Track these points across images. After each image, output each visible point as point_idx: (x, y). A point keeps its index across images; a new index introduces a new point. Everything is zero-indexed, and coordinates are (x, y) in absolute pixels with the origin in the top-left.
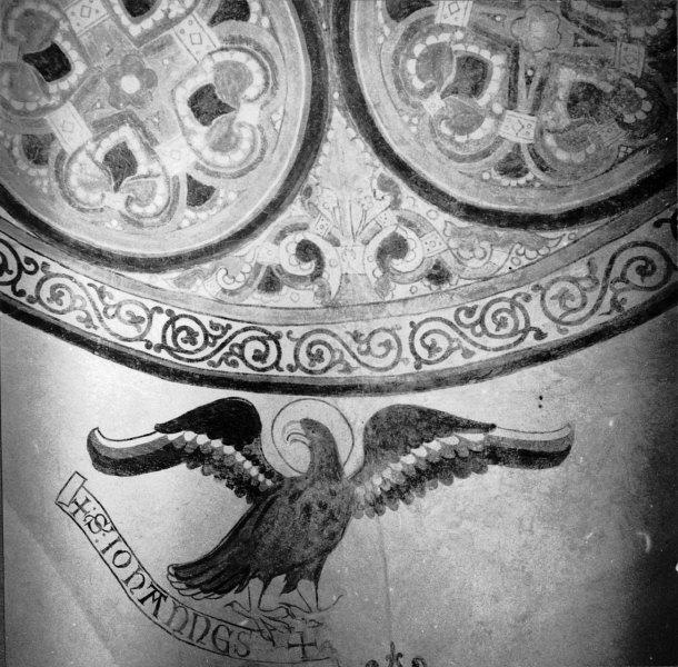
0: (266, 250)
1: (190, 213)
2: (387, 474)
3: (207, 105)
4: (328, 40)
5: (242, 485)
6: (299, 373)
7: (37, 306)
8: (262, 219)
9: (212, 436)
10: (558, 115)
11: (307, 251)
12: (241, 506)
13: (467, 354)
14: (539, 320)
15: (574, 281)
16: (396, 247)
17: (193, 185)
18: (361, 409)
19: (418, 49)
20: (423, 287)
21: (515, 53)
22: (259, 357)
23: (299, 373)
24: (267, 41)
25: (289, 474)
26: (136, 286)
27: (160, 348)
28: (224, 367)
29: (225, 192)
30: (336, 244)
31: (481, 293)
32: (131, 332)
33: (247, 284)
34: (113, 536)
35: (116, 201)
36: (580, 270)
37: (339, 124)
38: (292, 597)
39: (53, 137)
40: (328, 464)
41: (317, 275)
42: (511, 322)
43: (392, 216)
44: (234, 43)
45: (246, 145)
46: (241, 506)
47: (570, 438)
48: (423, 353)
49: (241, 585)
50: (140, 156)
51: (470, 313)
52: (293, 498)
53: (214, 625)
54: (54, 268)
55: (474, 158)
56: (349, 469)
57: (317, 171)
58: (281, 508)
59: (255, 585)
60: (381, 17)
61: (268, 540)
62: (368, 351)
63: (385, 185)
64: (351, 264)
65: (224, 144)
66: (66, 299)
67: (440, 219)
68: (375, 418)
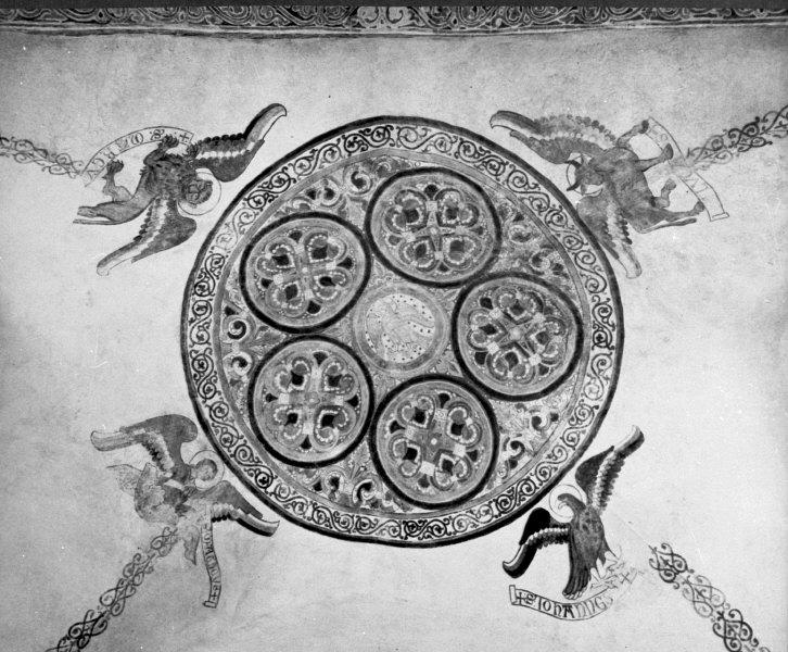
0: (505, 455)
1: (476, 464)
2: (597, 491)
3: (457, 428)
4: (472, 385)
5: (560, 539)
6: (544, 484)
10: (540, 348)
11: (515, 445)
12: (565, 547)
13: (584, 432)
14: (592, 404)
15: (589, 383)
16: (536, 421)
18: (570, 477)
19: (494, 365)
20: (554, 425)
22: (529, 489)
23: (544, 484)
24: (458, 399)
25: (569, 521)
26: (479, 500)
27: (500, 515)
28: (522, 503)
29: (480, 448)
30: (520, 435)
31: (570, 411)
32: (488, 517)
33: (507, 470)
34: (538, 599)
35: (454, 478)
36: (587, 379)
37: (493, 403)
38: (607, 563)
39: (425, 475)
40: (578, 506)
42: (586, 411)
43: (527, 414)
44: (451, 408)
46: (565, 547)
47: (638, 429)
48: (572, 444)
49: (589, 576)
51: (572, 419)
52: (577, 527)
53: (593, 599)
54: (453, 516)
55: (533, 377)
56: (585, 501)
57: (498, 420)
58: (579, 537)
59: (593, 571)
60: (479, 367)
61: (583, 550)
62: (557, 458)
63: (518, 407)
64: (529, 436)
65: (469, 436)
66: (464, 524)
67: (539, 402)
68: (577, 476)
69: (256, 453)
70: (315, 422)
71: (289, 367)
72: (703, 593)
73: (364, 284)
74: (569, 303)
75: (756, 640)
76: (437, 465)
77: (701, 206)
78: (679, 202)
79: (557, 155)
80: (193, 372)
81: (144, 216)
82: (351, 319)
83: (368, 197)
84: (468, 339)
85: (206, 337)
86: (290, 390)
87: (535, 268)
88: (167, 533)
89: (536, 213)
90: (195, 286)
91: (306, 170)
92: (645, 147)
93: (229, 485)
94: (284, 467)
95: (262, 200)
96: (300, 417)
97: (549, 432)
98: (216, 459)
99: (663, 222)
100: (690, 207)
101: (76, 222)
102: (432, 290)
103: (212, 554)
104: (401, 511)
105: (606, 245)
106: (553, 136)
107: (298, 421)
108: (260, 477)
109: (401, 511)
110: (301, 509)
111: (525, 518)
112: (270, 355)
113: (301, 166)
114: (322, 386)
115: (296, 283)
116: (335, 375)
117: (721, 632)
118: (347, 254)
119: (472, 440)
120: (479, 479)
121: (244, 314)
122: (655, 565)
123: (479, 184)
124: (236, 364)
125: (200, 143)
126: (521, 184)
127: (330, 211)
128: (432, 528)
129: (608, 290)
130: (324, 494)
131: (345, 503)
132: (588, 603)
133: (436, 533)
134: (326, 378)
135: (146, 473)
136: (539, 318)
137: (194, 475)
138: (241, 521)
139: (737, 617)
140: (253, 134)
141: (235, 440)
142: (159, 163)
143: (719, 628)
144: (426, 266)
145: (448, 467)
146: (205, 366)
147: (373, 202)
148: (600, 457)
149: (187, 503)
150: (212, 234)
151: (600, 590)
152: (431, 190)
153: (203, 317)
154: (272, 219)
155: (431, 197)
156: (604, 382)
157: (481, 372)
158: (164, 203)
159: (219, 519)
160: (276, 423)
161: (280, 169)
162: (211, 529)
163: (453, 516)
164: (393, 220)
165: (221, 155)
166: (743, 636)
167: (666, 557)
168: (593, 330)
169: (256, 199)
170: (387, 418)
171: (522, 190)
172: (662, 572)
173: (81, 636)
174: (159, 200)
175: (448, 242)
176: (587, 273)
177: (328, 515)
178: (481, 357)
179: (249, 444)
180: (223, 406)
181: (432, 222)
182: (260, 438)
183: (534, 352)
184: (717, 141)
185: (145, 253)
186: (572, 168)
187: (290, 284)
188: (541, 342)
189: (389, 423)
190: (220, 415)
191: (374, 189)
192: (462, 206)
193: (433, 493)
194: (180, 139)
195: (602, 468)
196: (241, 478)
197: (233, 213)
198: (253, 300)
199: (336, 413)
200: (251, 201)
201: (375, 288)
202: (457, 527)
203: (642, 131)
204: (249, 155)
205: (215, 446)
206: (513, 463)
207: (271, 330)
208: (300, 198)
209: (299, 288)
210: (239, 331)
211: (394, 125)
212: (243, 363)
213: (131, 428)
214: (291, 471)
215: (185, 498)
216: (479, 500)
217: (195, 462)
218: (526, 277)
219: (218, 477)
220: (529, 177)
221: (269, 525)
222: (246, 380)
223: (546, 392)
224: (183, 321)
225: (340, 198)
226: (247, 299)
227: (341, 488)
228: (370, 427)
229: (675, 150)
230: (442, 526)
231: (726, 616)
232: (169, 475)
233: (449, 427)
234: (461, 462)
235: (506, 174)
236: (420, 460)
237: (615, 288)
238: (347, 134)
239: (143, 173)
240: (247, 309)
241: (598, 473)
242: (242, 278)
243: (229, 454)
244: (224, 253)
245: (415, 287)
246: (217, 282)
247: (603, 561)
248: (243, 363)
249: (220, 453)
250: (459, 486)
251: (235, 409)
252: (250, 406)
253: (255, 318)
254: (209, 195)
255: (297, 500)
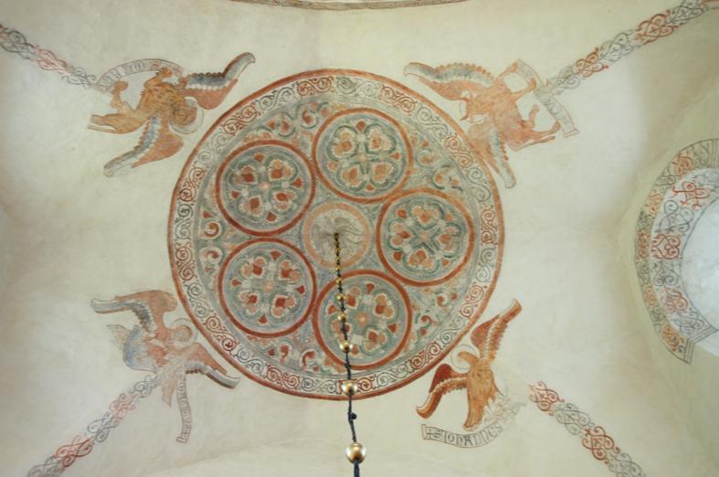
0: (416, 327)
3: (380, 309)
4: (391, 276)
5: (462, 385)
7: (381, 388)
8: (410, 321)
9: (443, 381)
11: (424, 318)
12: (464, 391)
13: (476, 306)
14: (482, 285)
16: (441, 299)
17: (390, 327)
18: (467, 339)
21: (424, 244)
22: (436, 351)
24: (381, 287)
25: (466, 371)
28: (431, 361)
30: (428, 311)
33: (418, 337)
34: (444, 433)
35: (378, 346)
36: (478, 267)
37: (407, 288)
38: (497, 401)
40: (474, 360)
41: (431, 320)
45: (393, 309)
48: (467, 315)
50: (376, 332)
51: (468, 297)
55: (437, 268)
56: (479, 356)
59: (486, 407)
62: (456, 326)
63: (426, 290)
65: (390, 312)
66: (386, 380)
68: (472, 339)
69: (223, 322)
70: (271, 303)
71: (251, 261)
72: (573, 417)
73: (310, 201)
74: (464, 210)
75: (617, 449)
76: (365, 337)
77: (557, 126)
78: (543, 123)
79: (450, 93)
80: (176, 260)
81: (139, 132)
82: (300, 228)
83: (315, 131)
84: (389, 244)
85: (187, 234)
86: (251, 277)
87: (438, 185)
88: (148, 379)
89: (438, 140)
90: (181, 192)
91: (268, 106)
92: (516, 83)
93: (201, 346)
94: (245, 336)
95: (235, 127)
96: (259, 298)
97: (450, 307)
98: (192, 326)
99: (531, 141)
100: (550, 128)
101: (90, 128)
102: (362, 206)
103: (184, 399)
104: (336, 373)
105: (489, 162)
106: (450, 80)
107: (258, 302)
108: (226, 343)
109: (336, 373)
110: (258, 369)
111: (432, 372)
112: (237, 250)
113: (265, 103)
114: (276, 276)
115: (259, 196)
116: (287, 269)
117: (589, 445)
118: (298, 176)
119: (392, 317)
120: (398, 344)
121: (218, 218)
122: (534, 399)
123: (397, 120)
124: (210, 257)
125: (189, 76)
126: (426, 118)
127: (286, 141)
128: (361, 384)
129: (491, 199)
130: (276, 359)
131: (293, 365)
132: (484, 433)
133: (364, 388)
134: (280, 271)
135: (135, 332)
136: (442, 223)
137: (172, 337)
138: (210, 376)
139: (601, 432)
140: (229, 74)
141: (207, 312)
142: (157, 88)
143: (587, 442)
144: (357, 186)
145: (373, 338)
146: (186, 256)
147: (318, 135)
148: (486, 325)
149: (166, 358)
150: (195, 152)
151: (492, 422)
152: (361, 125)
153: (186, 218)
154: (241, 144)
155: (360, 130)
156: (491, 268)
157: (398, 267)
158: (159, 120)
159: (192, 372)
160: (240, 303)
161: (249, 104)
162: (185, 380)
163: (377, 374)
164: (333, 150)
165: (204, 87)
166: (607, 446)
167: (541, 392)
168: (481, 231)
169: (230, 126)
170: (326, 303)
171: (428, 122)
172: (540, 404)
173: (68, 460)
174: (154, 118)
175: (374, 166)
176: (476, 186)
177: (279, 375)
178: (399, 255)
179: (217, 316)
180: (198, 286)
181: (362, 149)
182: (227, 311)
183: (438, 249)
184: (568, 71)
185: (143, 161)
186: (464, 103)
187: (254, 197)
188: (443, 242)
189: (327, 308)
190: (195, 293)
191: (319, 126)
192: (384, 137)
193: (361, 358)
194: (173, 72)
195: (491, 331)
196: (210, 341)
197: (212, 135)
198: (225, 207)
199: (286, 297)
200: (226, 127)
201: (318, 204)
202: (380, 383)
203: (513, 71)
204: (227, 90)
205: (191, 316)
206: (423, 331)
207: (238, 232)
208: (264, 128)
209: (260, 201)
210: (214, 231)
211: (334, 76)
212: (215, 256)
213: (124, 297)
214: (250, 339)
215: (165, 354)
216: (398, 362)
217: (174, 327)
218: (431, 192)
219: (192, 340)
220: (433, 112)
221: (233, 380)
222: (218, 268)
223: (447, 278)
224: (170, 220)
225: (294, 131)
226: (221, 206)
227: (290, 354)
228: (313, 309)
229: (538, 82)
230: (368, 382)
231: (592, 432)
232: (152, 335)
233: (374, 309)
234: (384, 333)
235: (416, 110)
236: (352, 334)
237: (497, 198)
238: (299, 81)
239: (143, 94)
240: (220, 214)
241: (488, 335)
242: (218, 190)
243: (202, 322)
244: (205, 168)
245: (348, 203)
246: (198, 190)
247: (494, 399)
248: (215, 256)
249: (195, 322)
250: (383, 351)
251: (207, 289)
252: (220, 287)
253: (226, 222)
254: (194, 119)
255: (255, 362)
